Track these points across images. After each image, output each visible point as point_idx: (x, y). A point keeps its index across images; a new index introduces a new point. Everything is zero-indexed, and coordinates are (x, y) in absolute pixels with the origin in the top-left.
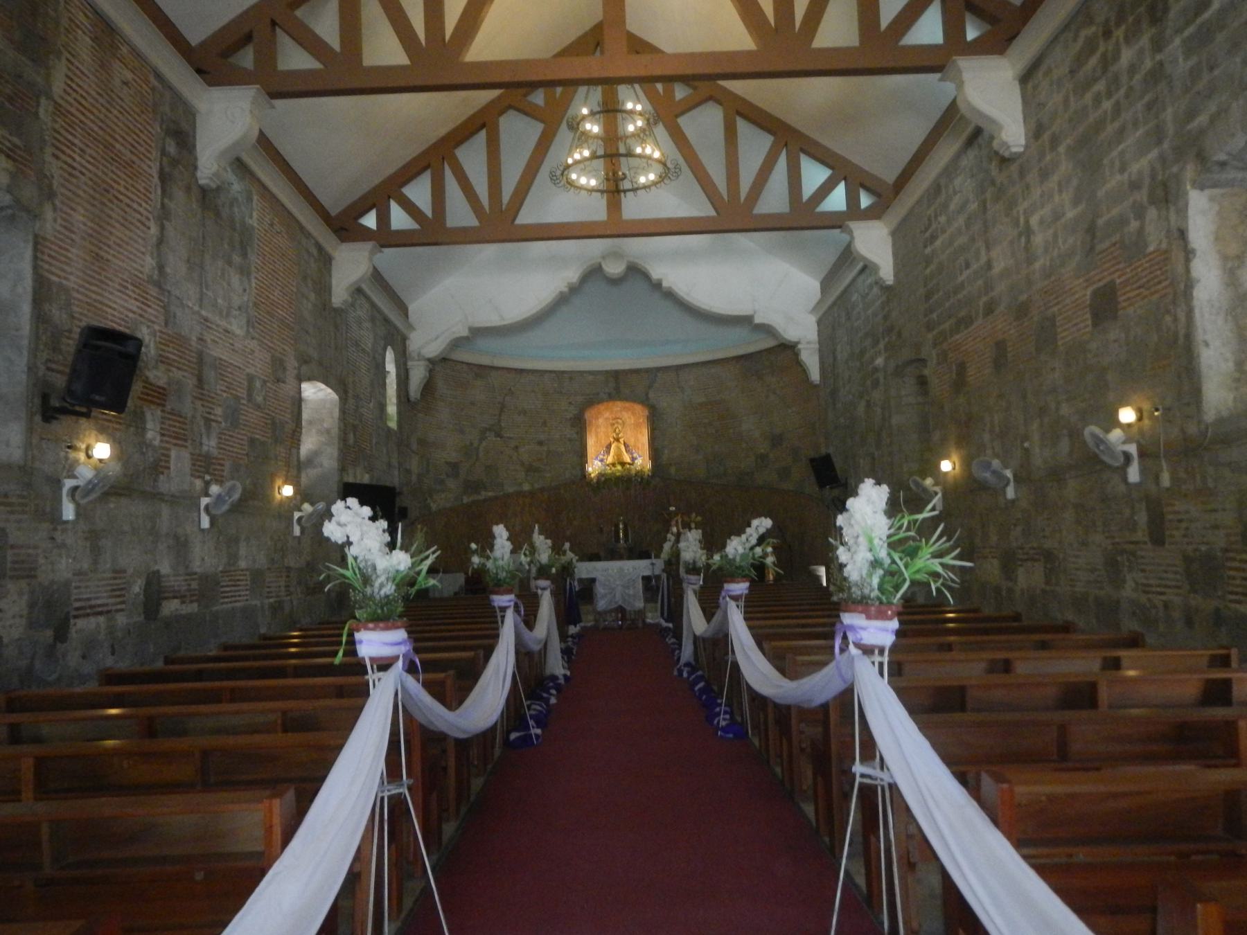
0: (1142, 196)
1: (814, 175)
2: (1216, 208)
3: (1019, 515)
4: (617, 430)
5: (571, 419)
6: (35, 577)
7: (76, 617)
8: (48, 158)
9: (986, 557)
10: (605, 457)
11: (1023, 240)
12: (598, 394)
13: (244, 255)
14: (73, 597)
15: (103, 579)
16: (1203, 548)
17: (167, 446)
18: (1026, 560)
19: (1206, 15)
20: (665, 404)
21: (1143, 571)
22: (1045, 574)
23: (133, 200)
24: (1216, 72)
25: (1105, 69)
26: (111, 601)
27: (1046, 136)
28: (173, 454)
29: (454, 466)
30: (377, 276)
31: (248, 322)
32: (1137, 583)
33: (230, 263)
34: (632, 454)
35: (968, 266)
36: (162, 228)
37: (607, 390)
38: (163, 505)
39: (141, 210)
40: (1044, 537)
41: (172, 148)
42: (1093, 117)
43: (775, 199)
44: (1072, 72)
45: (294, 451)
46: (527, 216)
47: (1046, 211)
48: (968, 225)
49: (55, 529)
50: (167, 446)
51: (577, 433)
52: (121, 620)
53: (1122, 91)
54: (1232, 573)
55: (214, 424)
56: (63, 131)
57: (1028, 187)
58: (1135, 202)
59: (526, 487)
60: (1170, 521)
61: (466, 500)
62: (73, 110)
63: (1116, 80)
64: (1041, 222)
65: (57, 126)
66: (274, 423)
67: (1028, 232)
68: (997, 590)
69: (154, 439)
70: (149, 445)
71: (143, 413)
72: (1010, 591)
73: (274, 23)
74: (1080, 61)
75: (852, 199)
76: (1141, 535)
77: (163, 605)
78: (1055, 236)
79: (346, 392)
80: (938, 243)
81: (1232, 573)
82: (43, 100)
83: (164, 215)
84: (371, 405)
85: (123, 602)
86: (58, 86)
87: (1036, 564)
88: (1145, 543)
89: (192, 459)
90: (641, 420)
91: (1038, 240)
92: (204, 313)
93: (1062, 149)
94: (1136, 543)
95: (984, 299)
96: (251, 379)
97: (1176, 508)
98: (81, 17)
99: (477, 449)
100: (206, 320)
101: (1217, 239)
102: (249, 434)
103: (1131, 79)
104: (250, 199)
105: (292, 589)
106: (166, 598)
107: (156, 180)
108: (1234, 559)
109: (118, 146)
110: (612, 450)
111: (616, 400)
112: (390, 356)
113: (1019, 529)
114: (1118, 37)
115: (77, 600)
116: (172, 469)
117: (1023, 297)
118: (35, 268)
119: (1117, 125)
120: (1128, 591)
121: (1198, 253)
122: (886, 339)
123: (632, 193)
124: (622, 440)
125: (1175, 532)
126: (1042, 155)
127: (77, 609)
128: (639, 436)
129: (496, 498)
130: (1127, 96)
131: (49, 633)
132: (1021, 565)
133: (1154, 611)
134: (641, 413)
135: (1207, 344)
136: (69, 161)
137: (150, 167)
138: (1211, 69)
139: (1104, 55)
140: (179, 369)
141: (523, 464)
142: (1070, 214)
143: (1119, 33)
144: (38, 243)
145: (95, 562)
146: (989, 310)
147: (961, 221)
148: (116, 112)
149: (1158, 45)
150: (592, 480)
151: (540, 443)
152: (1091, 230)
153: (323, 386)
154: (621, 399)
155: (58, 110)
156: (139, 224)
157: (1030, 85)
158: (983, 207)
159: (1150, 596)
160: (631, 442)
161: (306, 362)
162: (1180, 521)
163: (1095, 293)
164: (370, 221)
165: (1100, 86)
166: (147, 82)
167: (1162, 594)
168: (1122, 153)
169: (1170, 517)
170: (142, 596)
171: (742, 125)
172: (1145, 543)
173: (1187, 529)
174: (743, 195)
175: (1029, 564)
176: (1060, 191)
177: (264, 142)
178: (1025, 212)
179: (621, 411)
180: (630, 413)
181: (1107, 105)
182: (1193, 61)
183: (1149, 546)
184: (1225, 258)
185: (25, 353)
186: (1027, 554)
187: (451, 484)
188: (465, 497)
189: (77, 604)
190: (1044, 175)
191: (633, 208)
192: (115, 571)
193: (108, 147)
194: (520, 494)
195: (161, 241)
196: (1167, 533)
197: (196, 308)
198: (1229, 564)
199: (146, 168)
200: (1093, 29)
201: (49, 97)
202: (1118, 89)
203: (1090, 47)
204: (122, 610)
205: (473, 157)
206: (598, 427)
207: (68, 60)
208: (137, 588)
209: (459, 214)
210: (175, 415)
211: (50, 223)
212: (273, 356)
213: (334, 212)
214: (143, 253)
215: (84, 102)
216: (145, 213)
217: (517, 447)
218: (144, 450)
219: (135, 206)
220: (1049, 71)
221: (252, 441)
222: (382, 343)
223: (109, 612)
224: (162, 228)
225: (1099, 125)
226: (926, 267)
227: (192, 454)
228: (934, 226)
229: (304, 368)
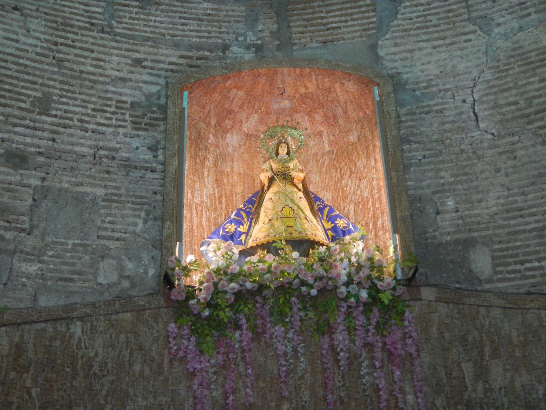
4: (283, 151)
5: (134, 105)
10: (243, 229)
12: (225, 48)
20: (433, 70)
34: (332, 219)
37: (251, 38)
51: (153, 149)
90: (353, 138)
110: (267, 204)
111: (280, 63)
124: (298, 176)
128: (348, 183)
134: (353, 114)
150: (191, 292)
154: (293, 63)
160: (327, 197)
179: (294, 111)
180: (318, 117)
206: (222, 157)
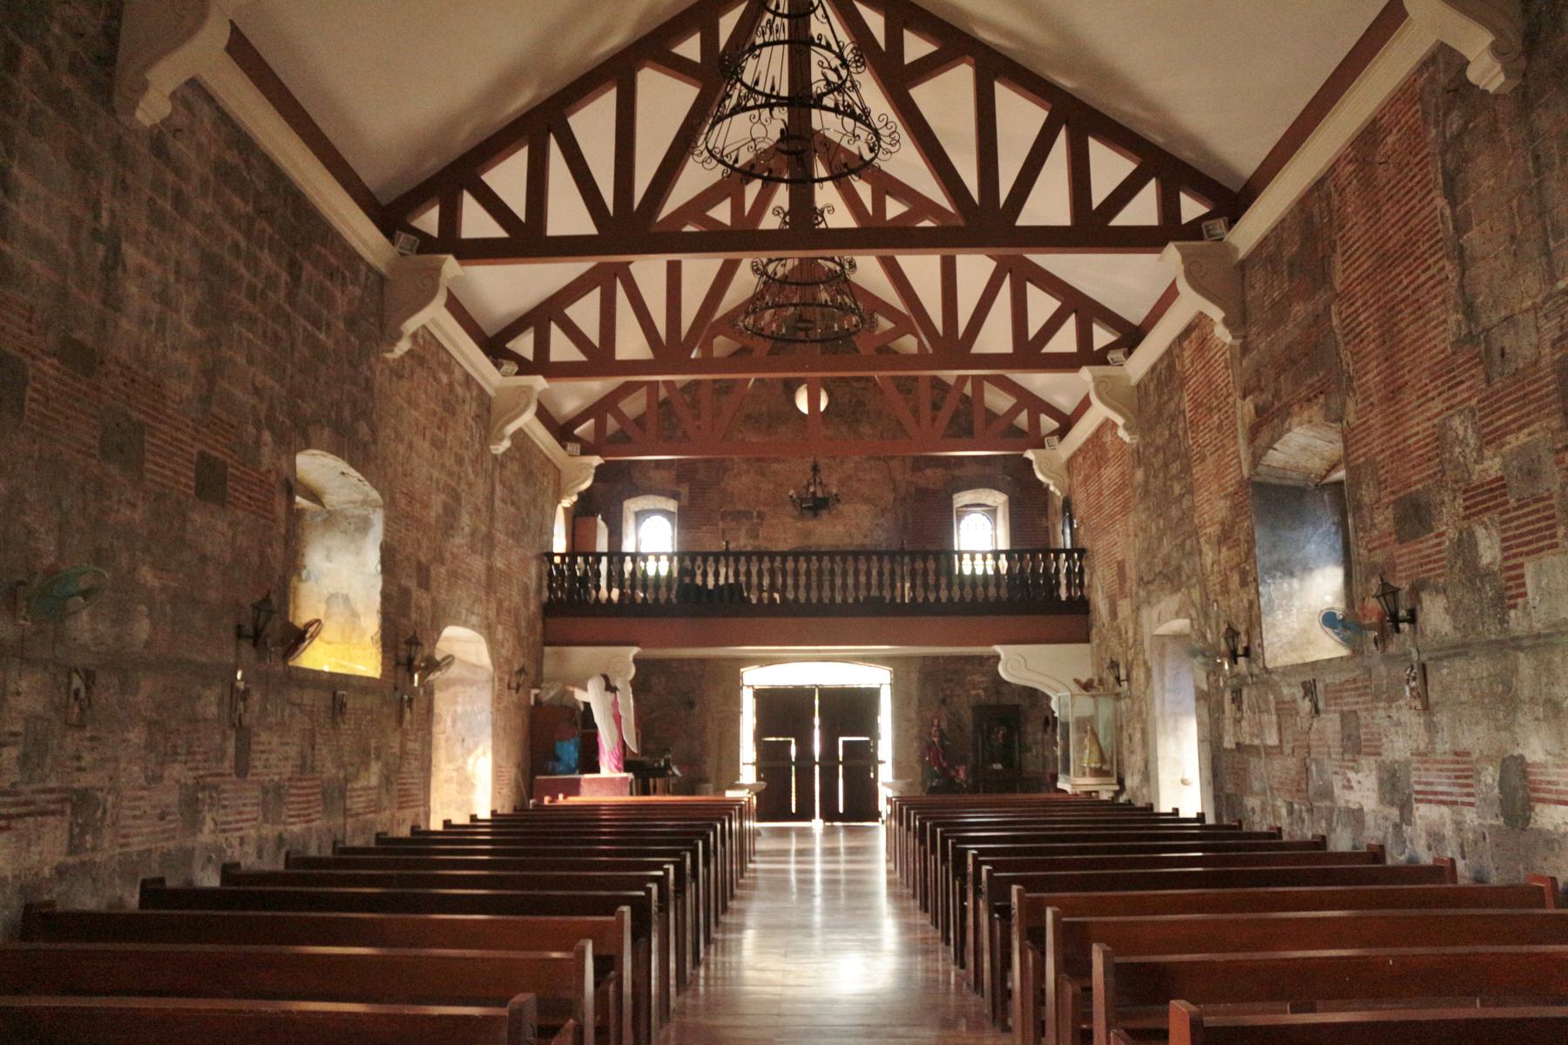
3: (18, 728)
6: (1379, 754)
7: (1421, 801)
14: (1413, 779)
15: (1443, 762)
16: (276, 778)
18: (20, 816)
21: (224, 807)
22: (72, 836)
26: (1456, 790)
32: (216, 824)
38: (1521, 655)
40: (79, 769)
52: (1470, 817)
70: (1487, 574)
76: (227, 766)
77: (1537, 810)
85: (1468, 795)
87: (51, 820)
88: (230, 775)
106: (1543, 801)
115: (1419, 783)
116: (1530, 596)
120: (206, 836)
125: (257, 763)
127: (1418, 792)
132: (8, 828)
133: (229, 852)
145: (1431, 742)
159: (227, 835)
162: (262, 752)
170: (1497, 791)
172: (230, 775)
173: (267, 760)
175: (30, 820)
186: (26, 803)
189: (1417, 788)
192: (1456, 754)
204: (1471, 804)
208: (1490, 776)
210: (1527, 505)
215: (1393, 220)
218: (1479, 584)
223: (1454, 803)
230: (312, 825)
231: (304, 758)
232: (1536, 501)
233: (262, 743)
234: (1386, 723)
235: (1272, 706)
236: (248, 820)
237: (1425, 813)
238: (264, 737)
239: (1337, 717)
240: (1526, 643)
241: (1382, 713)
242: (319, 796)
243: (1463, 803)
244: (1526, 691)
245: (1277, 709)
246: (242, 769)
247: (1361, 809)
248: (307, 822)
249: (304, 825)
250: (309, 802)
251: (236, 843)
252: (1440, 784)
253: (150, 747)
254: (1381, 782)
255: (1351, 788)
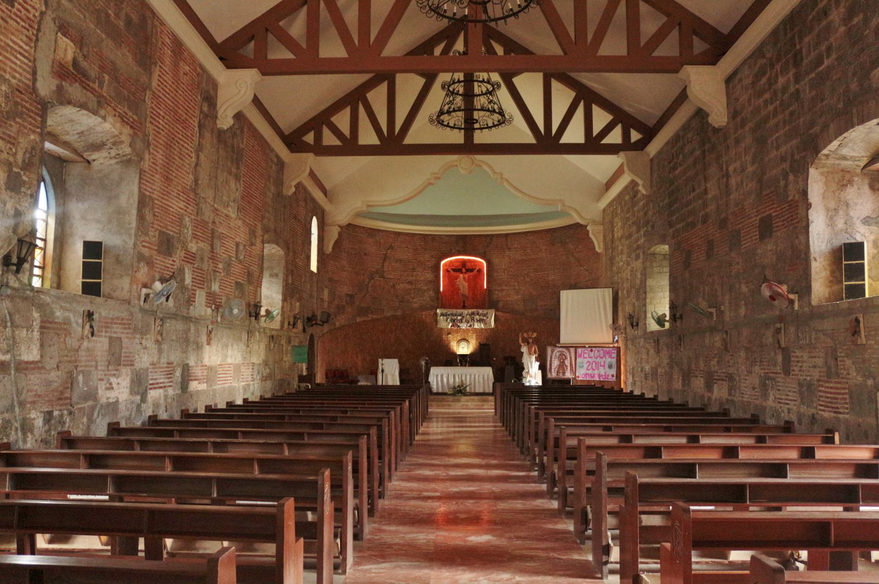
0: (786, 166)
1: (601, 117)
2: (824, 180)
6: (133, 365)
7: (150, 389)
8: (148, 125)
9: (697, 377)
11: (725, 179)
13: (238, 168)
14: (150, 377)
15: (163, 368)
16: (808, 378)
17: (194, 288)
19: (820, 69)
21: (779, 390)
23: (185, 142)
24: (824, 103)
25: (770, 85)
26: (167, 380)
27: (738, 119)
28: (197, 293)
29: (351, 296)
30: (312, 174)
31: (238, 209)
33: (230, 173)
35: (694, 190)
36: (198, 157)
37: (457, 248)
39: (189, 148)
40: (729, 366)
41: (205, 109)
42: (763, 113)
43: (574, 134)
44: (753, 83)
45: (259, 289)
46: (410, 139)
47: (737, 164)
48: (695, 164)
49: (142, 338)
50: (194, 288)
52: (171, 392)
53: (778, 102)
54: (822, 394)
55: (218, 274)
56: (156, 108)
57: (728, 147)
58: (783, 169)
59: (399, 313)
60: (794, 361)
61: (358, 320)
62: (161, 95)
63: (775, 93)
64: (735, 170)
65: (153, 105)
66: (249, 272)
67: (728, 176)
68: (703, 396)
69: (189, 284)
71: (184, 269)
72: (709, 399)
73: (267, 30)
74: (758, 77)
75: (626, 135)
76: (778, 369)
78: (742, 181)
79: (288, 248)
80: (677, 172)
81: (822, 394)
82: (148, 92)
83: (199, 148)
84: (302, 257)
85: (171, 382)
86: (154, 83)
88: (780, 373)
89: (207, 296)
91: (733, 181)
92: (216, 206)
93: (747, 128)
94: (776, 373)
95: (702, 213)
96: (237, 245)
97: (797, 354)
98: (168, 40)
99: (367, 285)
100: (217, 210)
101: (824, 198)
102: (236, 280)
103: (783, 96)
104: (242, 131)
105: (255, 377)
106: (191, 380)
107: (197, 129)
108: (822, 386)
109: (179, 111)
112: (314, 222)
113: (716, 360)
114: (777, 70)
115: (152, 379)
117: (723, 216)
118: (140, 188)
119: (776, 120)
120: (770, 402)
121: (813, 206)
122: (645, 229)
123: (479, 131)
125: (795, 368)
126: (736, 130)
129: (379, 320)
130: (781, 105)
131: (138, 398)
133: (783, 415)
135: (815, 260)
136: (157, 124)
137: (194, 121)
138: (822, 100)
139: (769, 79)
140: (202, 241)
141: (397, 296)
142: (750, 169)
143: (778, 67)
144: (142, 172)
145: (159, 358)
146: (705, 220)
147: (691, 160)
148: (180, 92)
149: (797, 79)
151: (410, 283)
152: (760, 181)
153: (276, 246)
155: (155, 96)
156: (187, 156)
157: (731, 85)
158: (704, 152)
161: (268, 232)
162: (798, 362)
163: (761, 219)
164: (310, 138)
165: (767, 96)
166: (195, 70)
167: (787, 404)
168: (777, 138)
169: (793, 359)
170: (180, 378)
171: (555, 85)
172: (780, 373)
173: (801, 367)
174: (554, 132)
176: (745, 155)
177: (257, 101)
178: (726, 162)
181: (771, 108)
182: (814, 93)
183: (782, 375)
184: (828, 210)
185: (133, 238)
187: (349, 309)
188: (358, 318)
189: (151, 382)
190: (737, 142)
191: (480, 138)
192: (168, 363)
193: (176, 112)
194: (394, 317)
195: (197, 165)
196: (792, 368)
197: (212, 203)
198: (821, 388)
199: (192, 121)
200: (765, 60)
201: (151, 90)
202: (776, 100)
203: (762, 72)
204: (171, 386)
205: (378, 97)
207: (160, 66)
209: (368, 137)
211: (146, 164)
212: (250, 229)
213: (287, 133)
214: (188, 173)
216: (190, 149)
217: (394, 285)
219: (186, 145)
220: (740, 80)
221: (237, 283)
222: (310, 214)
223: (165, 387)
224: (198, 157)
225: (767, 119)
226: (670, 186)
227: (206, 293)
228: (675, 160)
229: (266, 237)
230: (841, 416)
231: (829, 368)
232: (201, 270)
233: (797, 357)
234: (139, 347)
235: (36, 324)
236: (791, 400)
237: (153, 394)
238: (798, 353)
239: (106, 341)
240: (193, 320)
241: (137, 341)
242: (847, 396)
243: (168, 386)
244: (192, 339)
245: (42, 327)
246: (787, 371)
247: (117, 402)
248: (835, 412)
249: (833, 414)
250: (837, 399)
251: (786, 411)
252: (160, 379)
253: (747, 359)
254: (132, 381)
255: (113, 388)
